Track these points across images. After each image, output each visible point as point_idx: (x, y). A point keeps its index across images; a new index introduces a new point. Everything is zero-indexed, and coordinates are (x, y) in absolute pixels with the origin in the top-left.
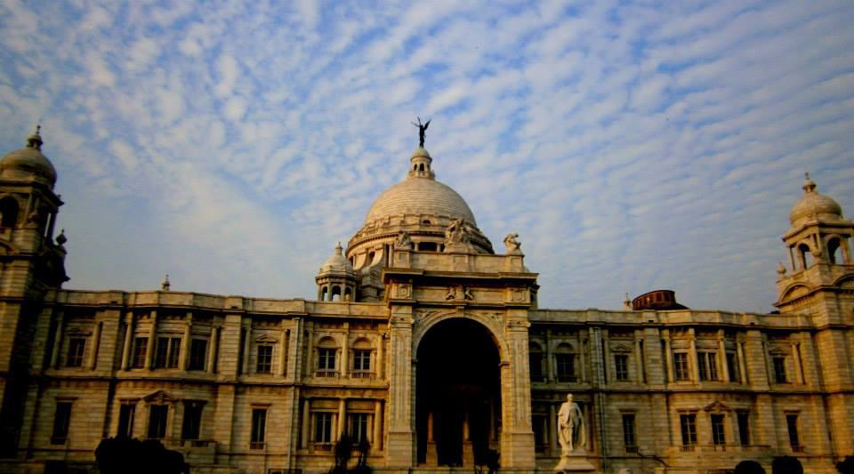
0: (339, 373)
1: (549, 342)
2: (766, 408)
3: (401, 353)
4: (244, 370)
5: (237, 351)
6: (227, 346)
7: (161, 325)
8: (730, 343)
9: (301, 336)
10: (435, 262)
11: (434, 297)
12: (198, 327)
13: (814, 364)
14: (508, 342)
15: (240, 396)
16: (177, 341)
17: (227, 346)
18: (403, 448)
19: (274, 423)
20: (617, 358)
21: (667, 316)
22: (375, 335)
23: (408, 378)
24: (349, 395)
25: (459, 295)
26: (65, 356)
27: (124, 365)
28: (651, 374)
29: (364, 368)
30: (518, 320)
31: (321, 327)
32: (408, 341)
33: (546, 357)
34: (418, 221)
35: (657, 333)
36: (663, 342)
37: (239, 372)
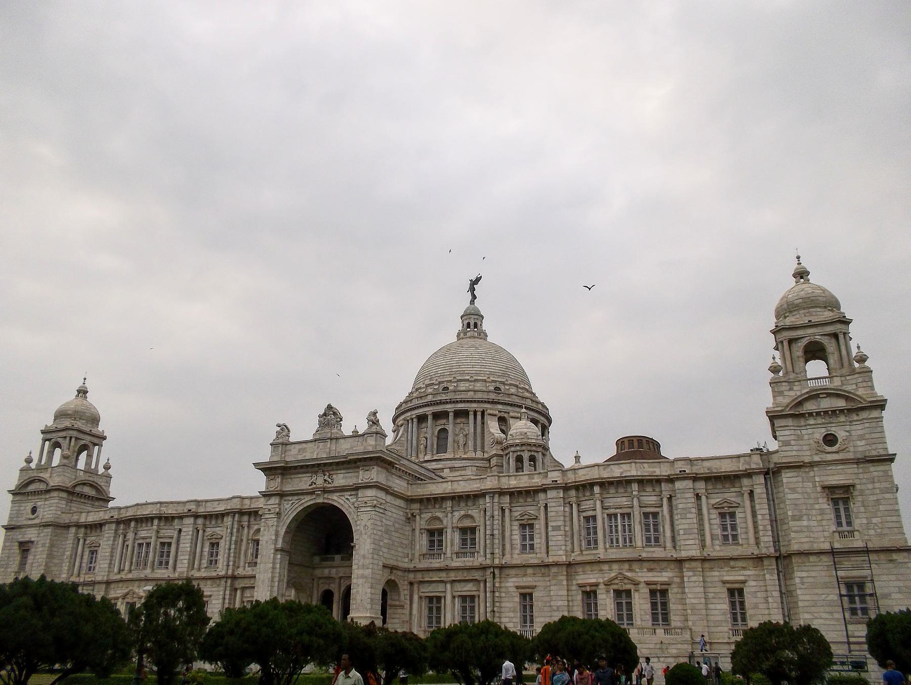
1: (450, 515)
3: (267, 542)
4: (196, 566)
5: (189, 549)
7: (139, 533)
8: (654, 498)
9: (235, 530)
10: (304, 450)
13: (768, 517)
16: (148, 544)
19: (212, 612)
20: (523, 526)
25: (320, 481)
26: (84, 565)
27: (116, 570)
30: (365, 499)
32: (273, 530)
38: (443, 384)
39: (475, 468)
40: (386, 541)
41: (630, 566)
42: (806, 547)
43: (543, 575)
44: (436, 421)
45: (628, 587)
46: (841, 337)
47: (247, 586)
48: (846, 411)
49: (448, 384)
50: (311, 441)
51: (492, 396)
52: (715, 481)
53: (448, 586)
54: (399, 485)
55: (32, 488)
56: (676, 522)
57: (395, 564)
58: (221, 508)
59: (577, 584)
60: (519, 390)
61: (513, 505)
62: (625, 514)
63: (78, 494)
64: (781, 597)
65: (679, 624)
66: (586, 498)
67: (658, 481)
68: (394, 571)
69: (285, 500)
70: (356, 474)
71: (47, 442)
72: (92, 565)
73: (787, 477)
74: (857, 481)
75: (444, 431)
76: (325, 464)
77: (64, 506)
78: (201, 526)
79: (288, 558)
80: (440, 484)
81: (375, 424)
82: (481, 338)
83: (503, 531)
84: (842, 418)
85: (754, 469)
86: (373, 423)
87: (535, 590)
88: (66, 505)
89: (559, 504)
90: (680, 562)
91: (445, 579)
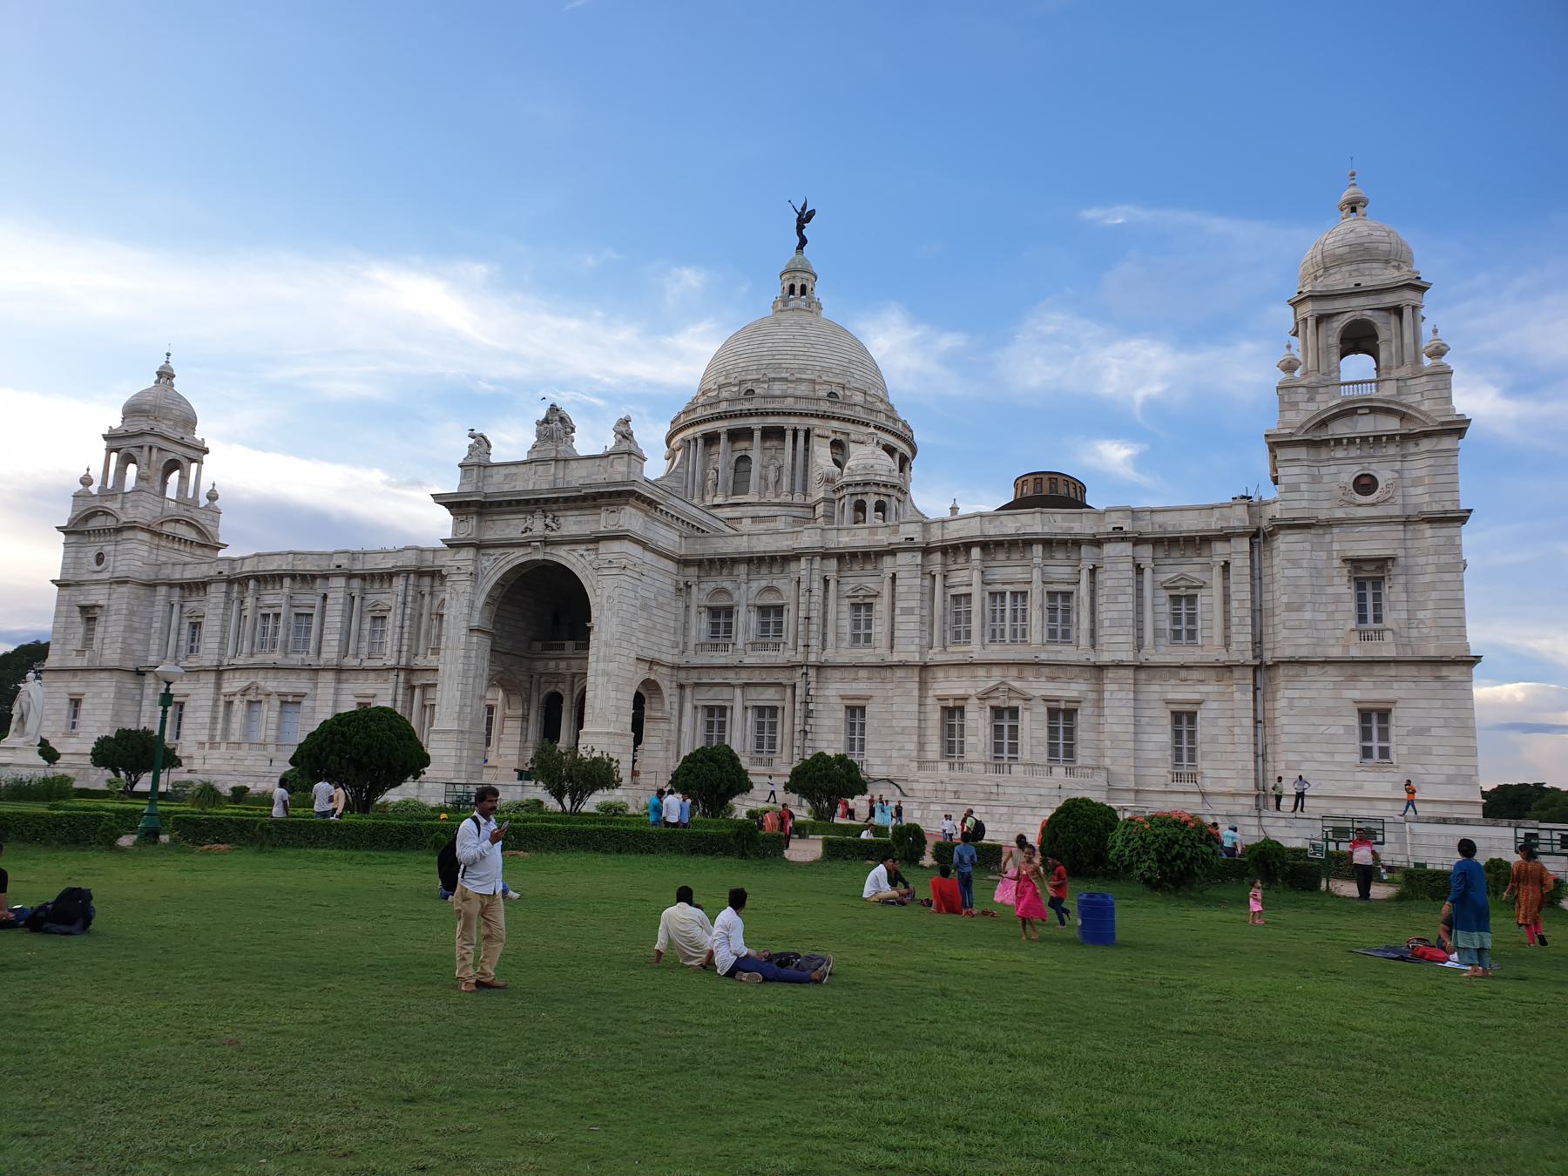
1: (744, 586)
2: (1121, 695)
3: (455, 617)
4: (350, 652)
5: (339, 625)
9: (410, 599)
12: (301, 597)
13: (1248, 604)
15: (344, 686)
16: (277, 616)
18: (444, 752)
20: (856, 607)
25: (538, 526)
26: (182, 643)
27: (230, 652)
30: (610, 557)
32: (464, 600)
35: (919, 559)
39: (791, 519)
40: (642, 622)
41: (1020, 672)
42: (1303, 652)
43: (883, 680)
44: (733, 443)
45: (1014, 703)
46: (1407, 313)
48: (1397, 438)
50: (524, 463)
51: (824, 407)
52: (1169, 545)
53: (738, 691)
54: (667, 537)
55: (95, 523)
56: (1100, 608)
57: (657, 656)
58: (388, 564)
60: (868, 398)
61: (843, 574)
62: (1017, 592)
63: (168, 536)
64: (1255, 727)
65: (1089, 762)
66: (958, 566)
67: (1074, 544)
68: (655, 668)
69: (483, 555)
70: (596, 517)
71: (114, 456)
72: (195, 645)
73: (1284, 542)
74: (1401, 553)
75: (745, 459)
76: (547, 500)
77: (146, 554)
78: (358, 591)
79: (487, 642)
80: (731, 538)
81: (627, 438)
82: (811, 312)
83: (825, 613)
84: (1392, 450)
85: (1235, 528)
86: (624, 437)
88: (150, 552)
89: (914, 574)
90: (1100, 668)
91: (733, 682)
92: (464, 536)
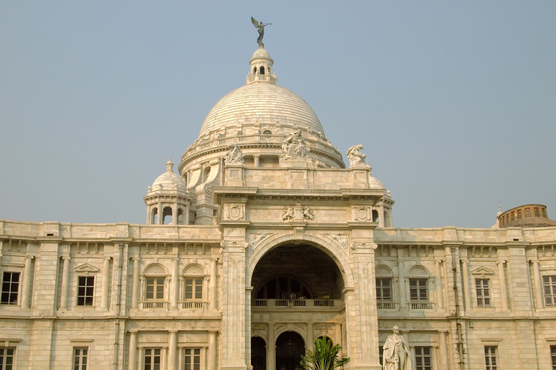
0: (169, 303)
1: (401, 264)
3: (233, 280)
4: (63, 303)
5: (54, 283)
6: (42, 278)
9: (125, 263)
10: (271, 179)
11: (269, 217)
12: (8, 258)
14: (352, 266)
15: (59, 333)
17: (42, 278)
19: (96, 359)
20: (478, 281)
21: (534, 234)
22: (208, 261)
23: (242, 307)
24: (180, 326)
25: (298, 215)
28: (516, 299)
29: (196, 297)
30: (363, 241)
31: (148, 253)
32: (241, 267)
33: (397, 281)
34: (257, 132)
35: (524, 254)
36: (530, 263)
37: (57, 306)
38: (265, 127)
47: (145, 329)
49: (271, 127)
59: (545, 338)
66: (547, 258)
87: (501, 343)
92: (236, 219)
